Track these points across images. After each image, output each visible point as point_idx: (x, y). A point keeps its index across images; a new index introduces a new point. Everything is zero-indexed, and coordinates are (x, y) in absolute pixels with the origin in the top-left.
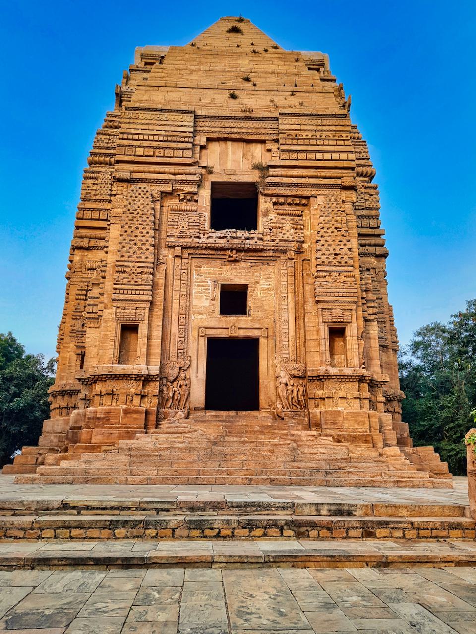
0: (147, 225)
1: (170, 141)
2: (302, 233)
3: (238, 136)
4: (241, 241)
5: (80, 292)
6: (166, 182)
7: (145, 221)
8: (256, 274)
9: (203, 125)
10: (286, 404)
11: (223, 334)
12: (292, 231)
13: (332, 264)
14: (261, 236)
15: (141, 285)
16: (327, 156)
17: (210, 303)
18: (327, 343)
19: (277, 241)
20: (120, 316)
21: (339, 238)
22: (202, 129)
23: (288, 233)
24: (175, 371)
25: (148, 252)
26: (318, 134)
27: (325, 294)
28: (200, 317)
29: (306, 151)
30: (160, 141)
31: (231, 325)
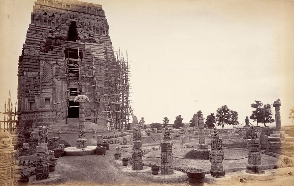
24: (60, 109)
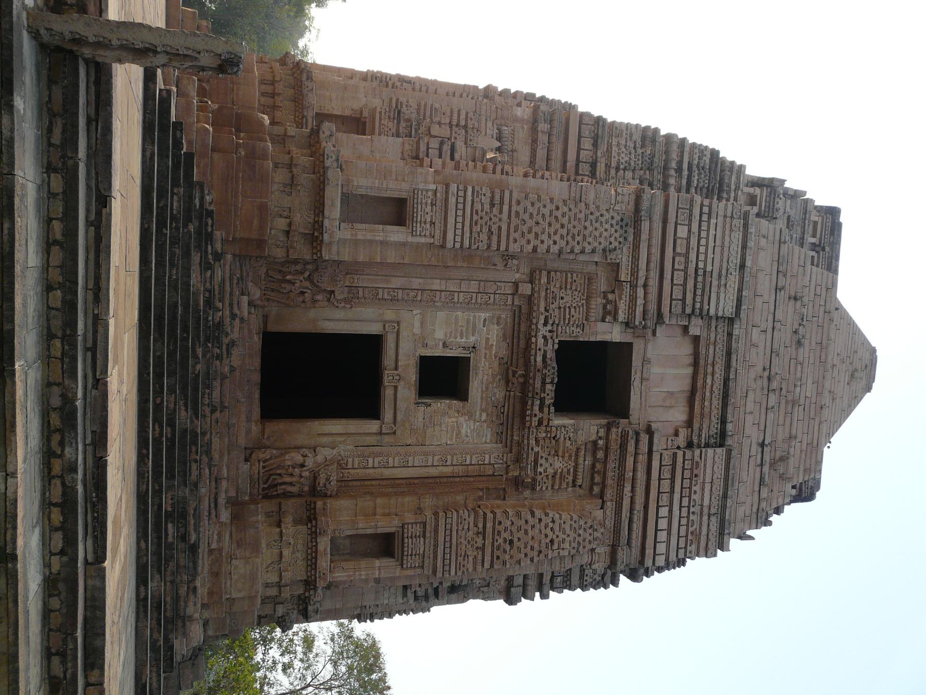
0: (567, 242)
1: (696, 278)
2: (547, 488)
3: (699, 384)
4: (539, 391)
5: (463, 116)
6: (634, 272)
7: (573, 238)
8: (484, 415)
9: (720, 331)
10: (272, 464)
11: (388, 360)
12: (550, 471)
13: (496, 537)
14: (545, 423)
15: (471, 233)
16: (663, 524)
17: (439, 340)
18: (369, 531)
19: (536, 449)
20: (420, 196)
21: (536, 546)
22: (713, 329)
23: (547, 465)
25: (524, 242)
26: (697, 509)
27: (448, 527)
28: (417, 324)
29: (672, 492)
30: (697, 264)
31: (403, 375)
